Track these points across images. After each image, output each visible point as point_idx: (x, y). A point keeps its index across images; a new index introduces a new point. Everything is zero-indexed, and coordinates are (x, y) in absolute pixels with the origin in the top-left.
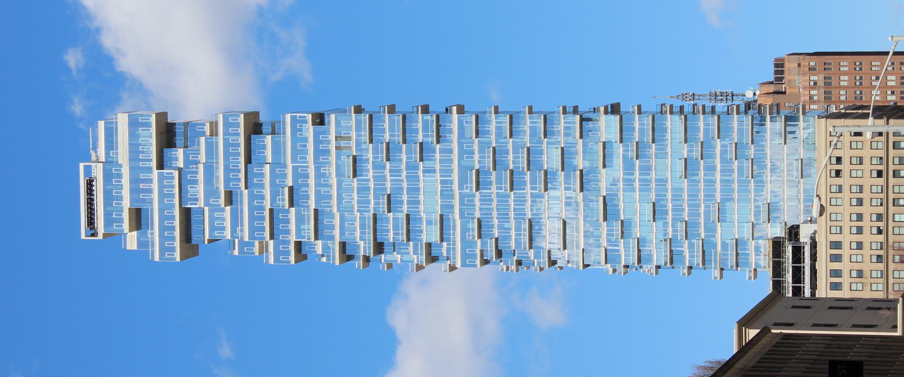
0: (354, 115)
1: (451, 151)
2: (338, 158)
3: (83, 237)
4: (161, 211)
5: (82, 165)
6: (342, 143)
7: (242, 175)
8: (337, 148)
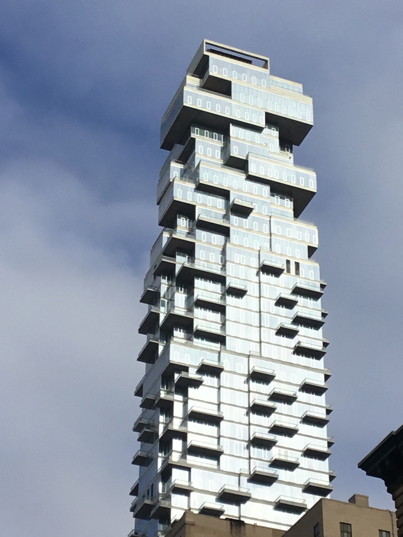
6: (293, 267)
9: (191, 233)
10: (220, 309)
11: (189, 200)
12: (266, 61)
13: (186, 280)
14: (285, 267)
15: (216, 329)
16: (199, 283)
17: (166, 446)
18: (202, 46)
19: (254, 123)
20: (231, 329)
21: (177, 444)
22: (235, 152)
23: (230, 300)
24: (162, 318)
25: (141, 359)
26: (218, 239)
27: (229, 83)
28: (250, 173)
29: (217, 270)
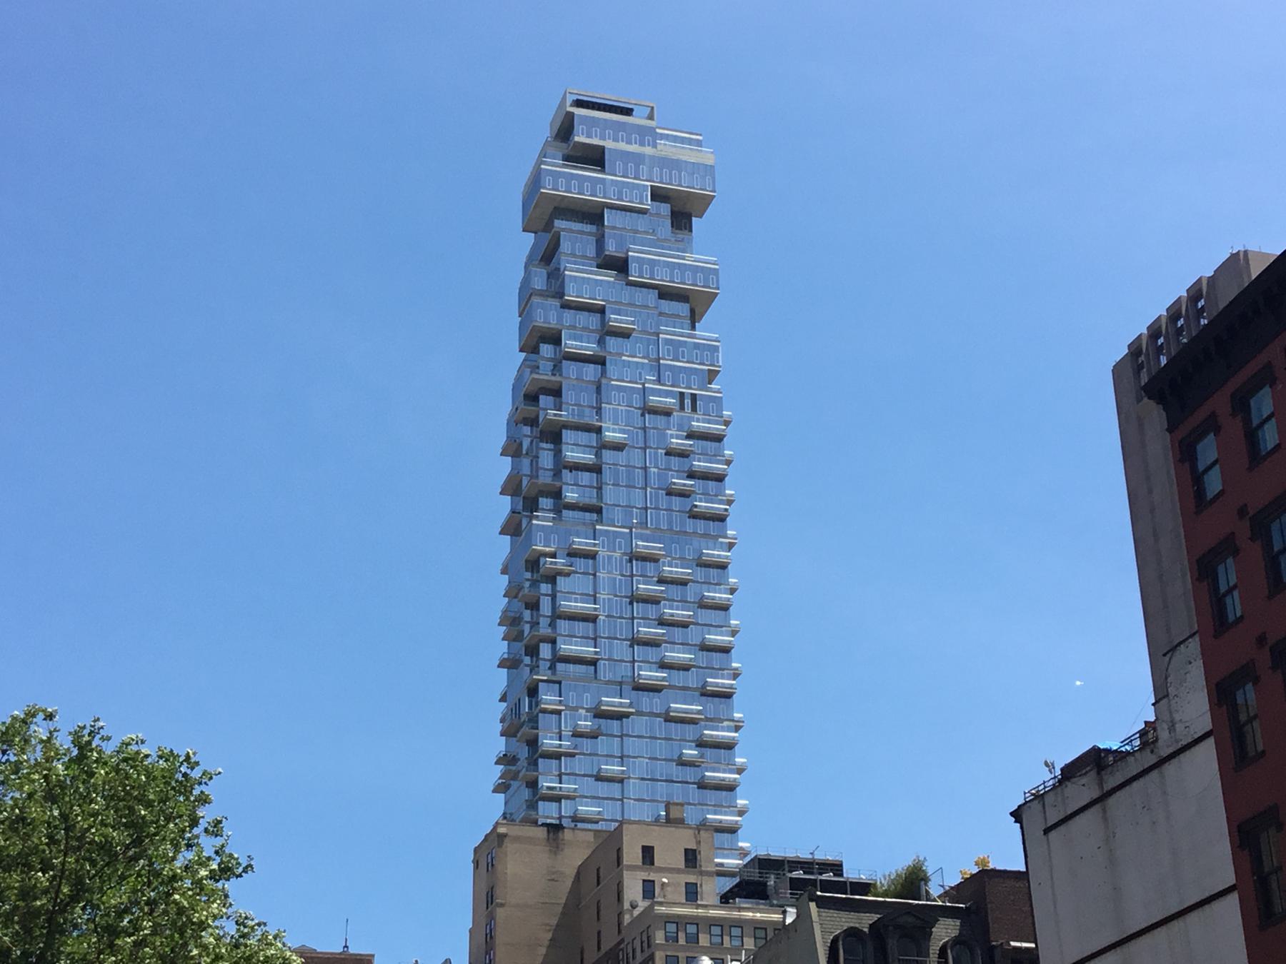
6: (688, 401)
8: (682, 394)
9: (557, 368)
10: (596, 469)
11: (553, 323)
13: (554, 435)
14: (677, 408)
15: (590, 498)
16: (568, 436)
17: (533, 651)
18: (564, 98)
20: (610, 495)
21: (545, 651)
22: (611, 248)
23: (608, 455)
24: (525, 482)
25: (503, 532)
26: (591, 371)
27: (603, 148)
29: (590, 418)
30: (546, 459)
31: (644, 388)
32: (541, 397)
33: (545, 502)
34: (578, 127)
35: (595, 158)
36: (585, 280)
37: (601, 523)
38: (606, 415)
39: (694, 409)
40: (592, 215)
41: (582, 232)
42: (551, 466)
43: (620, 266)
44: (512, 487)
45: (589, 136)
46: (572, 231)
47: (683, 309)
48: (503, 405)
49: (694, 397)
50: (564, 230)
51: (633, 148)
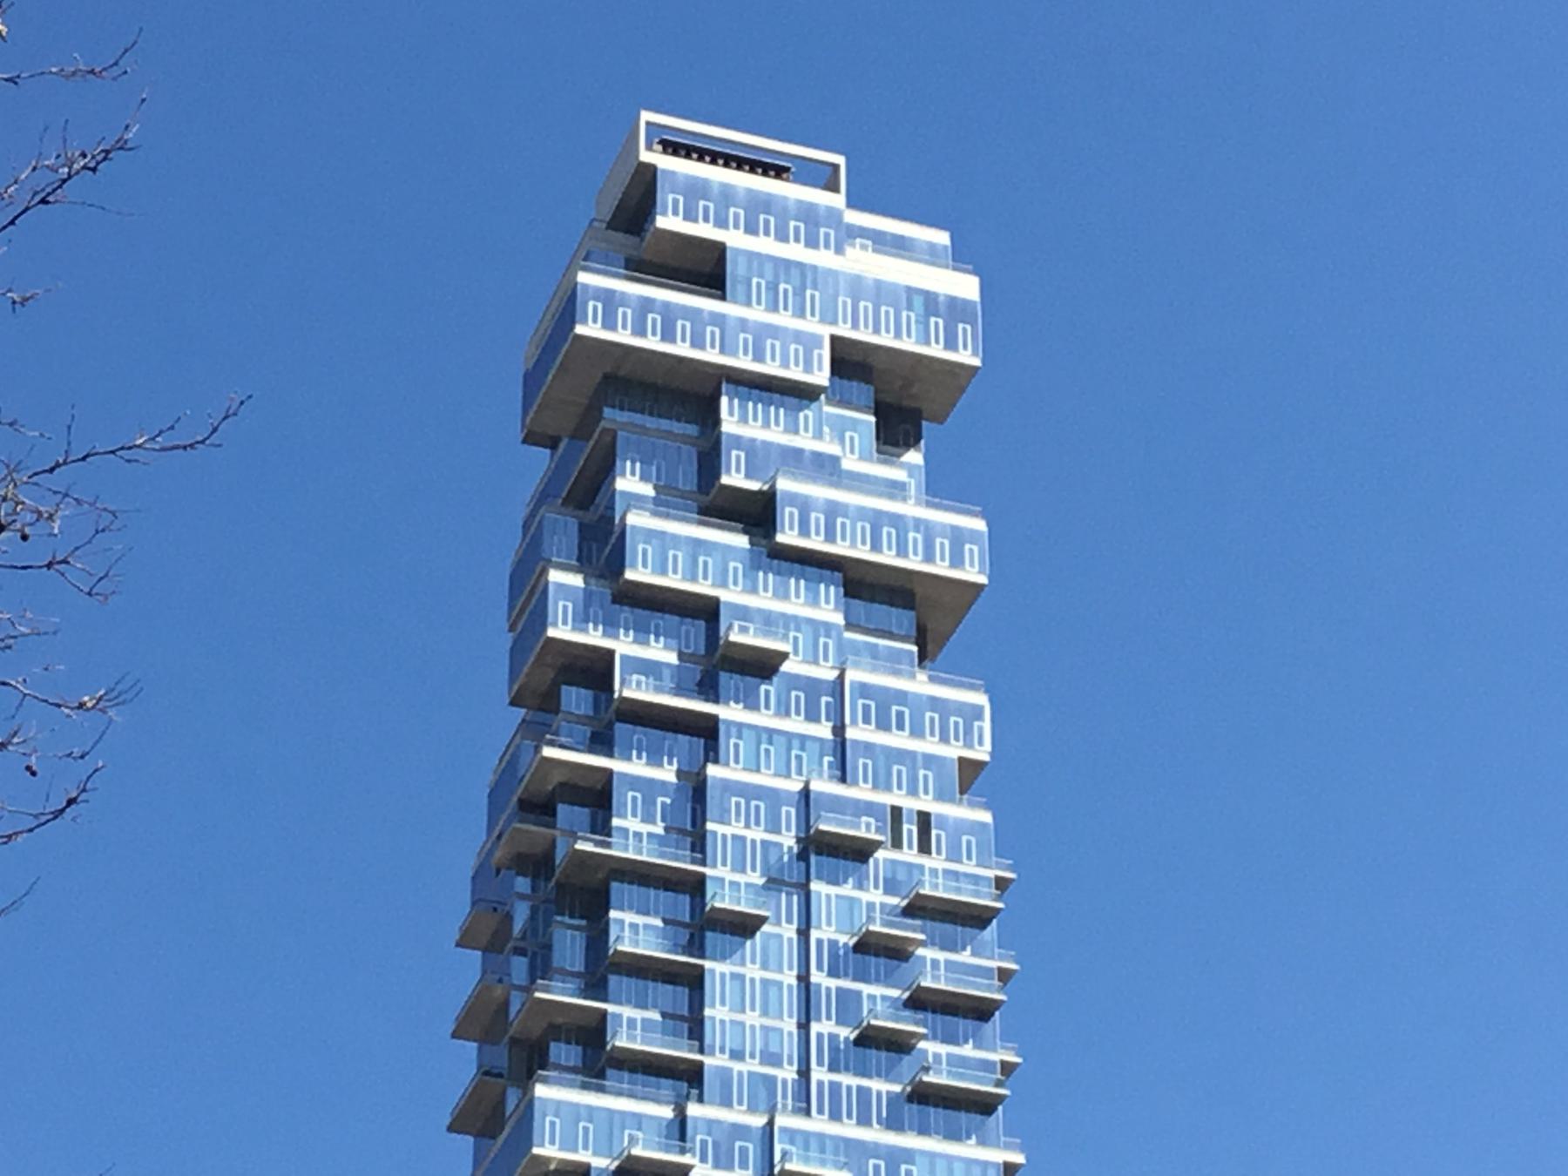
0: (991, 873)
1: (893, 1123)
2: (869, 808)
3: (646, 116)
4: (719, 320)
5: (839, 160)
6: (910, 829)
7: (816, 543)
8: (897, 812)
12: (836, 167)
19: (795, 374)
25: (457, 1126)
27: (719, 250)
28: (780, 538)
30: (569, 944)
31: (806, 793)
32: (562, 809)
33: (562, 1052)
34: (667, 197)
35: (705, 269)
36: (669, 545)
37: (700, 1100)
38: (715, 848)
39: (924, 848)
40: (690, 396)
41: (669, 434)
42: (579, 967)
43: (756, 514)
44: (482, 1021)
45: (690, 216)
46: (644, 430)
47: (904, 619)
48: (461, 836)
49: (924, 820)
50: (624, 426)
51: (795, 251)
